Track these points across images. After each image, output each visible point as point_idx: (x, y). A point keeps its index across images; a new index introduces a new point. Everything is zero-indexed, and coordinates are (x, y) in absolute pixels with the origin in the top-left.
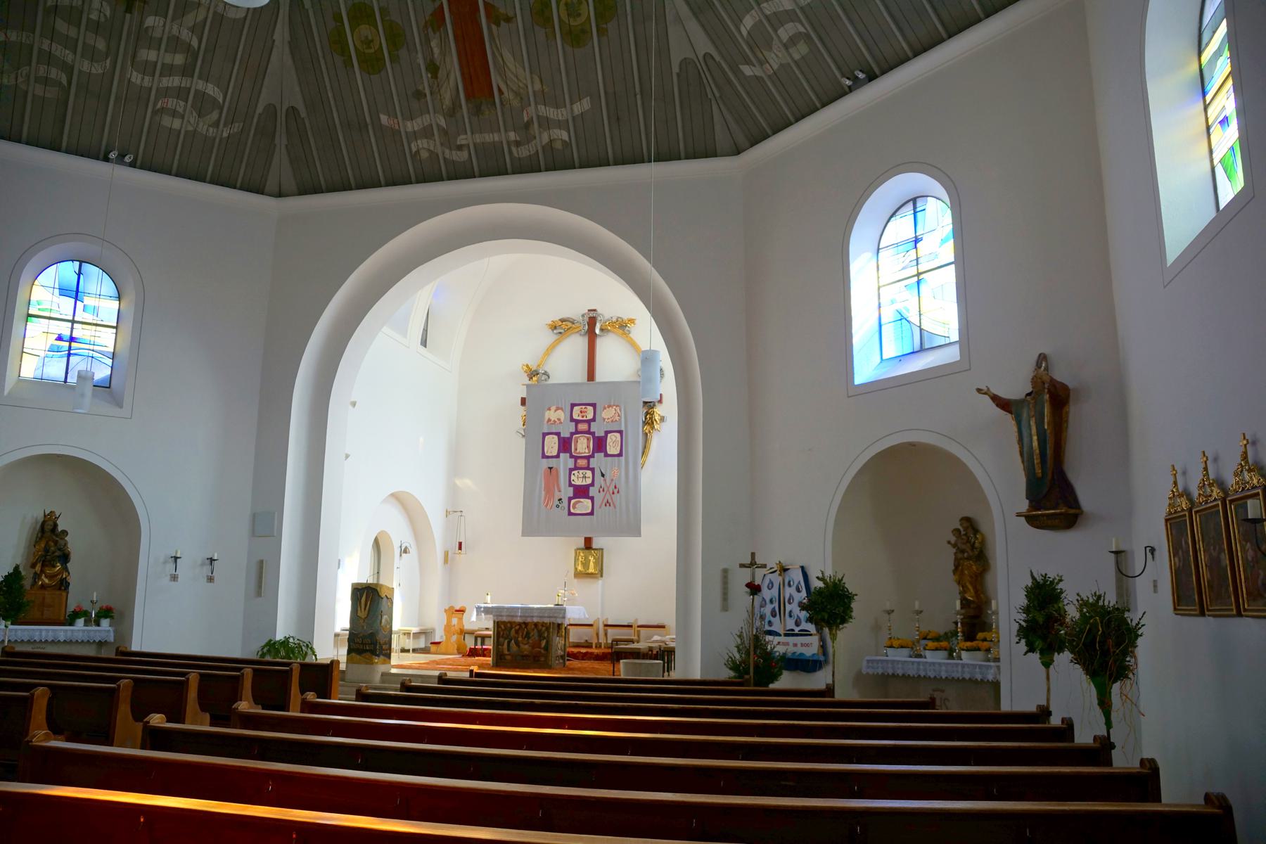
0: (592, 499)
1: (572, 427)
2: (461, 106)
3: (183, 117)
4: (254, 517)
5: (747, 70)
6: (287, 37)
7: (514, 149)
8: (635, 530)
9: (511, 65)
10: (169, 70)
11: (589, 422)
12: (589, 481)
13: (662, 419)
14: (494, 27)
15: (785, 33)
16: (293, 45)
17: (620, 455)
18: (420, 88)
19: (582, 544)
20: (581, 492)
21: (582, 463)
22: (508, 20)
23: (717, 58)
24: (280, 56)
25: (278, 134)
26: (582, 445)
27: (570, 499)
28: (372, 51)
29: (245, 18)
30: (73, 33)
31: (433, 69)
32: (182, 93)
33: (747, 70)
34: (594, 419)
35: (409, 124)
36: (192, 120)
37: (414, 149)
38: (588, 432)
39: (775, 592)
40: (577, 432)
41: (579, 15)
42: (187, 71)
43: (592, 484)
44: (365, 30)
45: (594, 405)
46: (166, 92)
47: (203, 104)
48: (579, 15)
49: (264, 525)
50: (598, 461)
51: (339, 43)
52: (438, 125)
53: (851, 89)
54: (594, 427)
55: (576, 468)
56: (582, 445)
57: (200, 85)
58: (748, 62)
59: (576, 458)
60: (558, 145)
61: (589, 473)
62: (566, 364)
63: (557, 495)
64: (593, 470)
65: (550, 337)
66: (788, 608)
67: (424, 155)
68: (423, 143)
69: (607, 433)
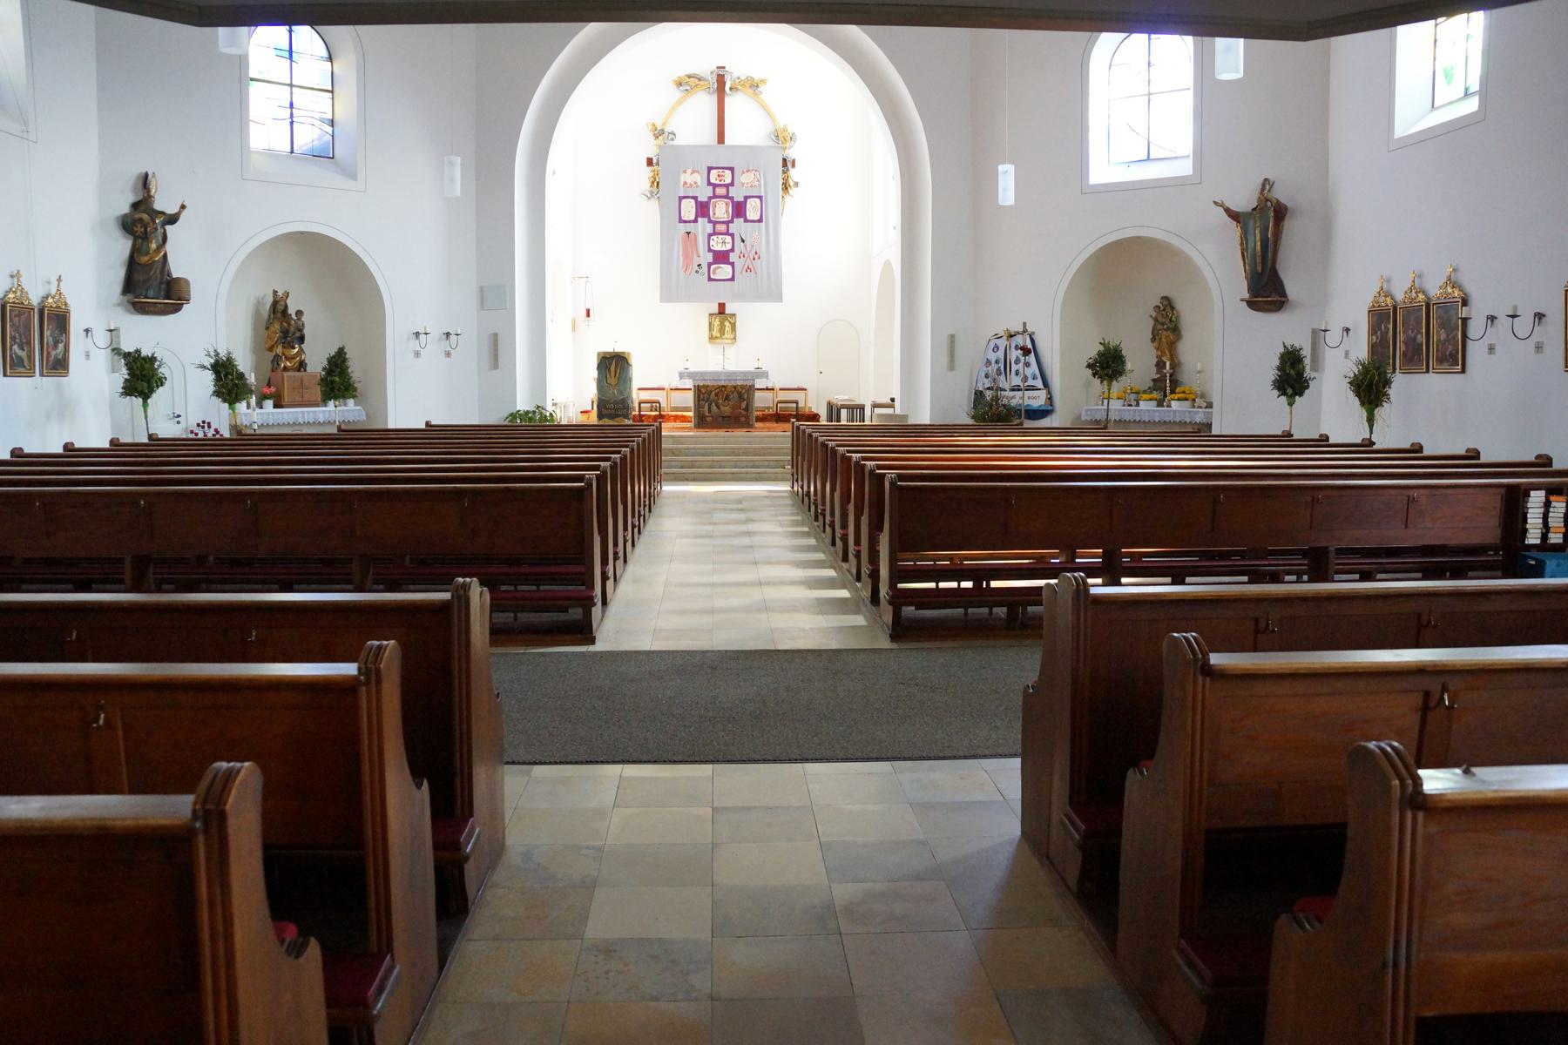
0: (733, 264)
1: (709, 191)
4: (482, 290)
8: (777, 296)
11: (727, 186)
12: (729, 247)
13: (796, 184)
17: (760, 221)
19: (716, 310)
20: (721, 257)
21: (722, 228)
26: (721, 210)
27: (709, 265)
34: (732, 184)
38: (727, 197)
39: (1001, 354)
40: (715, 196)
43: (732, 250)
45: (732, 169)
49: (493, 296)
50: (738, 226)
54: (732, 192)
55: (715, 233)
56: (721, 210)
59: (715, 223)
61: (729, 239)
62: (693, 123)
63: (696, 261)
64: (732, 235)
65: (676, 94)
66: (1014, 367)
69: (746, 198)
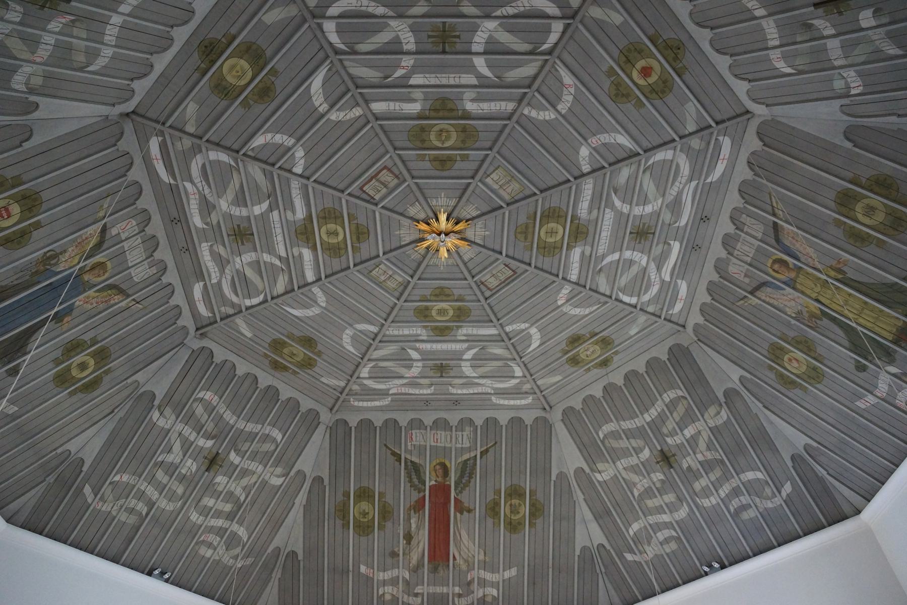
2: (423, 566)
3: (215, 549)
5: (629, 557)
6: (304, 502)
7: (456, 599)
9: (465, 542)
10: (218, 514)
14: (458, 515)
15: (661, 536)
16: (307, 508)
18: (396, 550)
22: (469, 511)
23: (608, 547)
24: (296, 515)
25: (276, 570)
28: (366, 520)
29: (281, 485)
30: (165, 480)
31: (409, 537)
32: (221, 532)
33: (629, 557)
35: (381, 574)
36: (220, 553)
37: (381, 592)
41: (518, 513)
42: (230, 517)
44: (364, 505)
46: (211, 530)
47: (232, 541)
48: (518, 513)
51: (342, 511)
52: (403, 577)
53: (706, 574)
57: (235, 527)
58: (631, 551)
60: (489, 599)
67: (388, 597)
68: (389, 589)
